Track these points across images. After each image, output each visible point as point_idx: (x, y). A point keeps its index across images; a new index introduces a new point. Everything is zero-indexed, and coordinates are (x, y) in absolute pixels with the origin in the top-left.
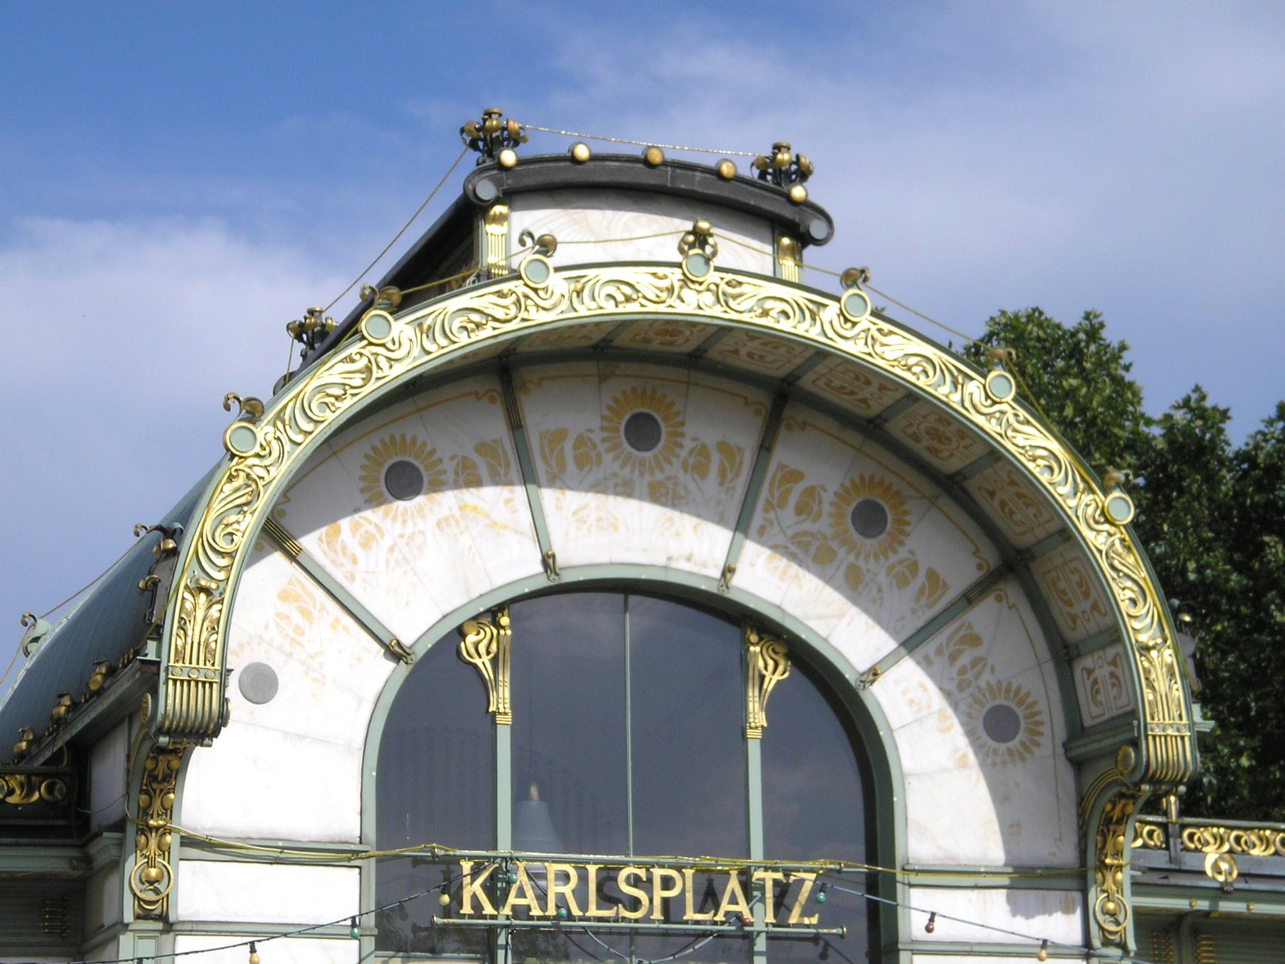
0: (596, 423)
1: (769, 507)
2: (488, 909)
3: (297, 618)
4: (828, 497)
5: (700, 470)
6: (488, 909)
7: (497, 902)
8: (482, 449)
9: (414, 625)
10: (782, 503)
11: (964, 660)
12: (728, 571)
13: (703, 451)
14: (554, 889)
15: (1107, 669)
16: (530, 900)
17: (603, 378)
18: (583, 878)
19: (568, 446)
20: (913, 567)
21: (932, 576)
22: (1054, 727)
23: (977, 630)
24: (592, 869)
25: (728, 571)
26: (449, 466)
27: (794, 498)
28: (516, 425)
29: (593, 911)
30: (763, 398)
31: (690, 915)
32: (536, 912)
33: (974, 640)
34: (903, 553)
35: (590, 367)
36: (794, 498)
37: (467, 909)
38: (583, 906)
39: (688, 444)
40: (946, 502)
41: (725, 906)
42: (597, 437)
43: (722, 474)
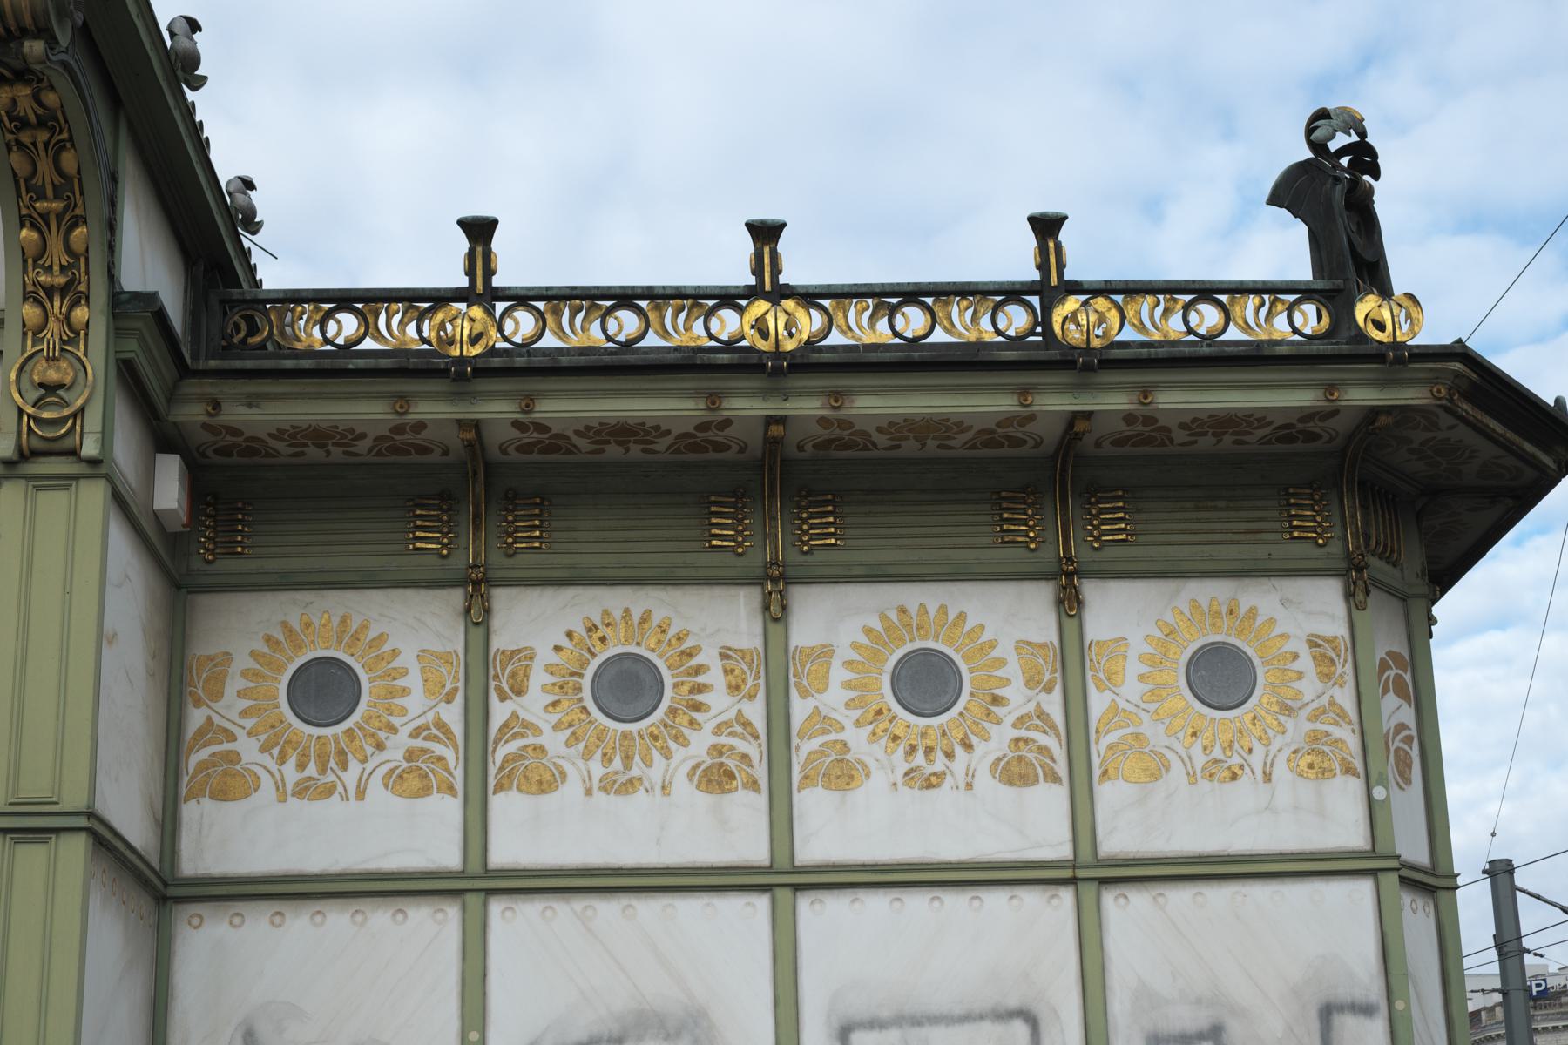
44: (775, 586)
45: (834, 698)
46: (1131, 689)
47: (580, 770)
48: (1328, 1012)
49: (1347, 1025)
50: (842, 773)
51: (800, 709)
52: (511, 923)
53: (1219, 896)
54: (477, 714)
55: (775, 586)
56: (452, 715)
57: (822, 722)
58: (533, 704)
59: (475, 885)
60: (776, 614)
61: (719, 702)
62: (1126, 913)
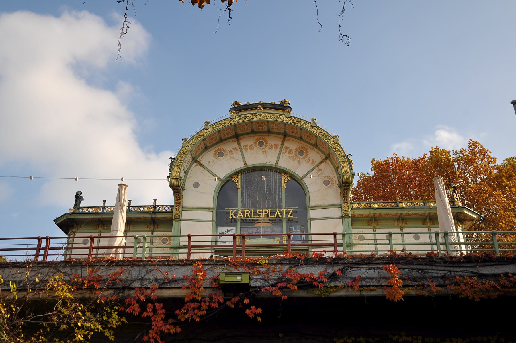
0: (253, 143)
2: (234, 217)
5: (271, 148)
6: (234, 217)
8: (234, 149)
10: (286, 152)
11: (320, 173)
12: (277, 163)
13: (272, 145)
14: (245, 214)
16: (242, 215)
17: (254, 136)
19: (248, 147)
20: (310, 160)
22: (336, 182)
23: (322, 168)
24: (252, 210)
25: (277, 163)
26: (228, 152)
27: (288, 151)
28: (239, 145)
29: (252, 216)
30: (282, 137)
31: (270, 216)
32: (242, 217)
33: (321, 170)
34: (308, 157)
35: (252, 135)
36: (288, 151)
37: (231, 217)
38: (250, 215)
39: (269, 145)
40: (315, 149)
41: (276, 215)
43: (275, 148)
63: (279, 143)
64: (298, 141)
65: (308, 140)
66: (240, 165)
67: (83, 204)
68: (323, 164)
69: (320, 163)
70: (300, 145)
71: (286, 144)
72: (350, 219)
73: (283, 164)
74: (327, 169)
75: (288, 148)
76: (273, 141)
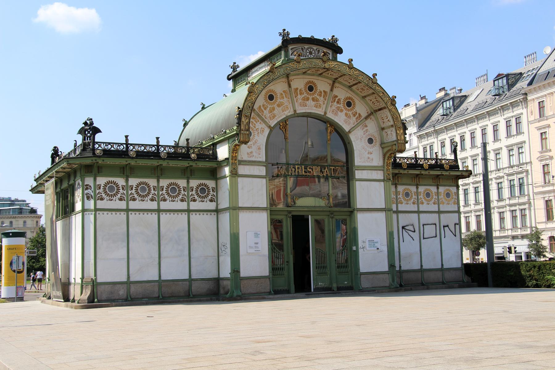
0: (303, 87)
1: (332, 102)
2: (287, 173)
3: (255, 122)
4: (342, 100)
7: (288, 173)
8: (284, 91)
9: (273, 123)
10: (334, 101)
15: (390, 132)
18: (302, 168)
20: (356, 113)
21: (359, 114)
27: (336, 100)
33: (366, 126)
34: (354, 110)
36: (336, 100)
39: (318, 91)
42: (303, 89)
44: (417, 186)
45: (422, 196)
46: (442, 196)
47: (404, 202)
48: (455, 224)
49: (457, 226)
50: (422, 203)
51: (419, 197)
52: (400, 215)
53: (448, 215)
54: (397, 197)
55: (417, 186)
56: (395, 197)
57: (421, 198)
58: (401, 196)
59: (397, 212)
60: (417, 188)
61: (414, 196)
62: (442, 215)
63: (328, 88)
64: (346, 89)
65: (358, 92)
66: (289, 112)
67: (98, 138)
68: (369, 120)
69: (366, 118)
70: (348, 95)
71: (336, 92)
72: (390, 182)
73: (330, 115)
74: (372, 127)
75: (336, 97)
76: (322, 85)
